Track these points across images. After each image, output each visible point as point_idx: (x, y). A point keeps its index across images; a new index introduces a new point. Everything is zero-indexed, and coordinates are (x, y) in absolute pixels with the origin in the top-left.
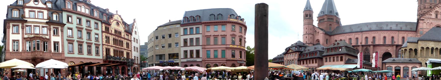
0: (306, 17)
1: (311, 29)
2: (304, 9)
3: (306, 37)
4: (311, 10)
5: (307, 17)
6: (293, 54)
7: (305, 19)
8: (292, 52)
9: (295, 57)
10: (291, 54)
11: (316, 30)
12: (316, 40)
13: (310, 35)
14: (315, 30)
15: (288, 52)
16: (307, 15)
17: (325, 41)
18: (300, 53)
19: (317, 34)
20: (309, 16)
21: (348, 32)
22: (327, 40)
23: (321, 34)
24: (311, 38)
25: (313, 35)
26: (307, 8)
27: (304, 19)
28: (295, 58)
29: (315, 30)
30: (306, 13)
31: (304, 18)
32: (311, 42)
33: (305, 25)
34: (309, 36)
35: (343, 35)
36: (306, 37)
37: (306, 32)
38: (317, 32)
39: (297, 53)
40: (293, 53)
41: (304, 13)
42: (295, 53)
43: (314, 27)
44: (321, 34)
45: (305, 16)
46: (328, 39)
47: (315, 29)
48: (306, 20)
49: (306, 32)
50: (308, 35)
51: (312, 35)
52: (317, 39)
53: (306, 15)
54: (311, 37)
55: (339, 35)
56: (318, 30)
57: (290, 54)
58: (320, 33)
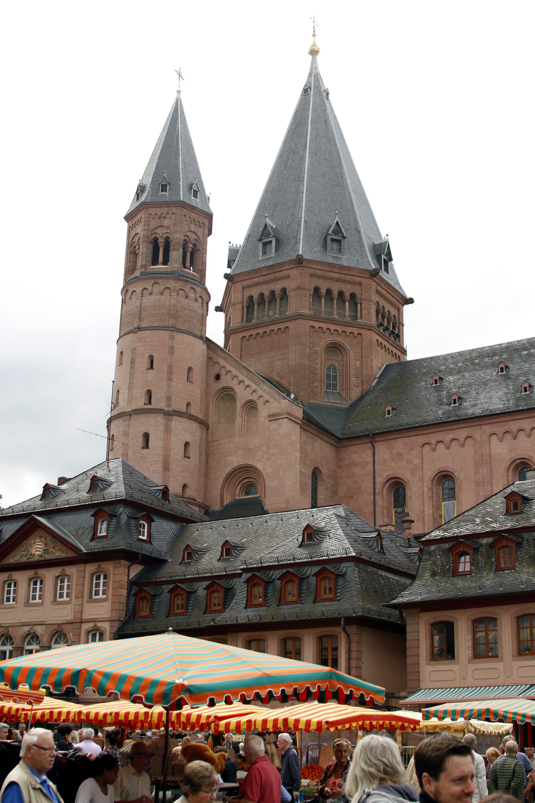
0: (155, 262)
1: (190, 369)
2: (141, 189)
3: (146, 436)
4: (196, 202)
5: (166, 262)
6: (61, 578)
7: (146, 276)
8: (58, 554)
9: (86, 606)
10: (42, 572)
11: (233, 384)
12: (229, 469)
13: (177, 423)
14: (226, 381)
15: (14, 558)
16: (167, 241)
17: (302, 490)
18: (136, 570)
19: (238, 421)
20: (176, 255)
21: (497, 405)
22: (316, 474)
23: (274, 417)
24: (186, 456)
25: (204, 424)
26: (164, 188)
27: (128, 282)
28: (86, 617)
29: (226, 381)
30: (154, 223)
31: (130, 269)
32: (185, 486)
33: (139, 329)
34: (168, 430)
35: (461, 433)
36: (146, 436)
37: (149, 393)
38: (239, 403)
39: (109, 566)
40: (71, 570)
41: (139, 229)
42: (91, 568)
43: (210, 358)
44: (274, 417)
45: (144, 250)
46: (324, 471)
47: (218, 377)
48: (148, 285)
49: (149, 393)
50: (160, 419)
51: (195, 426)
52: (242, 462)
53: (155, 243)
54: (187, 444)
55: (421, 440)
56: (247, 382)
57: (30, 573)
58: (264, 412)
